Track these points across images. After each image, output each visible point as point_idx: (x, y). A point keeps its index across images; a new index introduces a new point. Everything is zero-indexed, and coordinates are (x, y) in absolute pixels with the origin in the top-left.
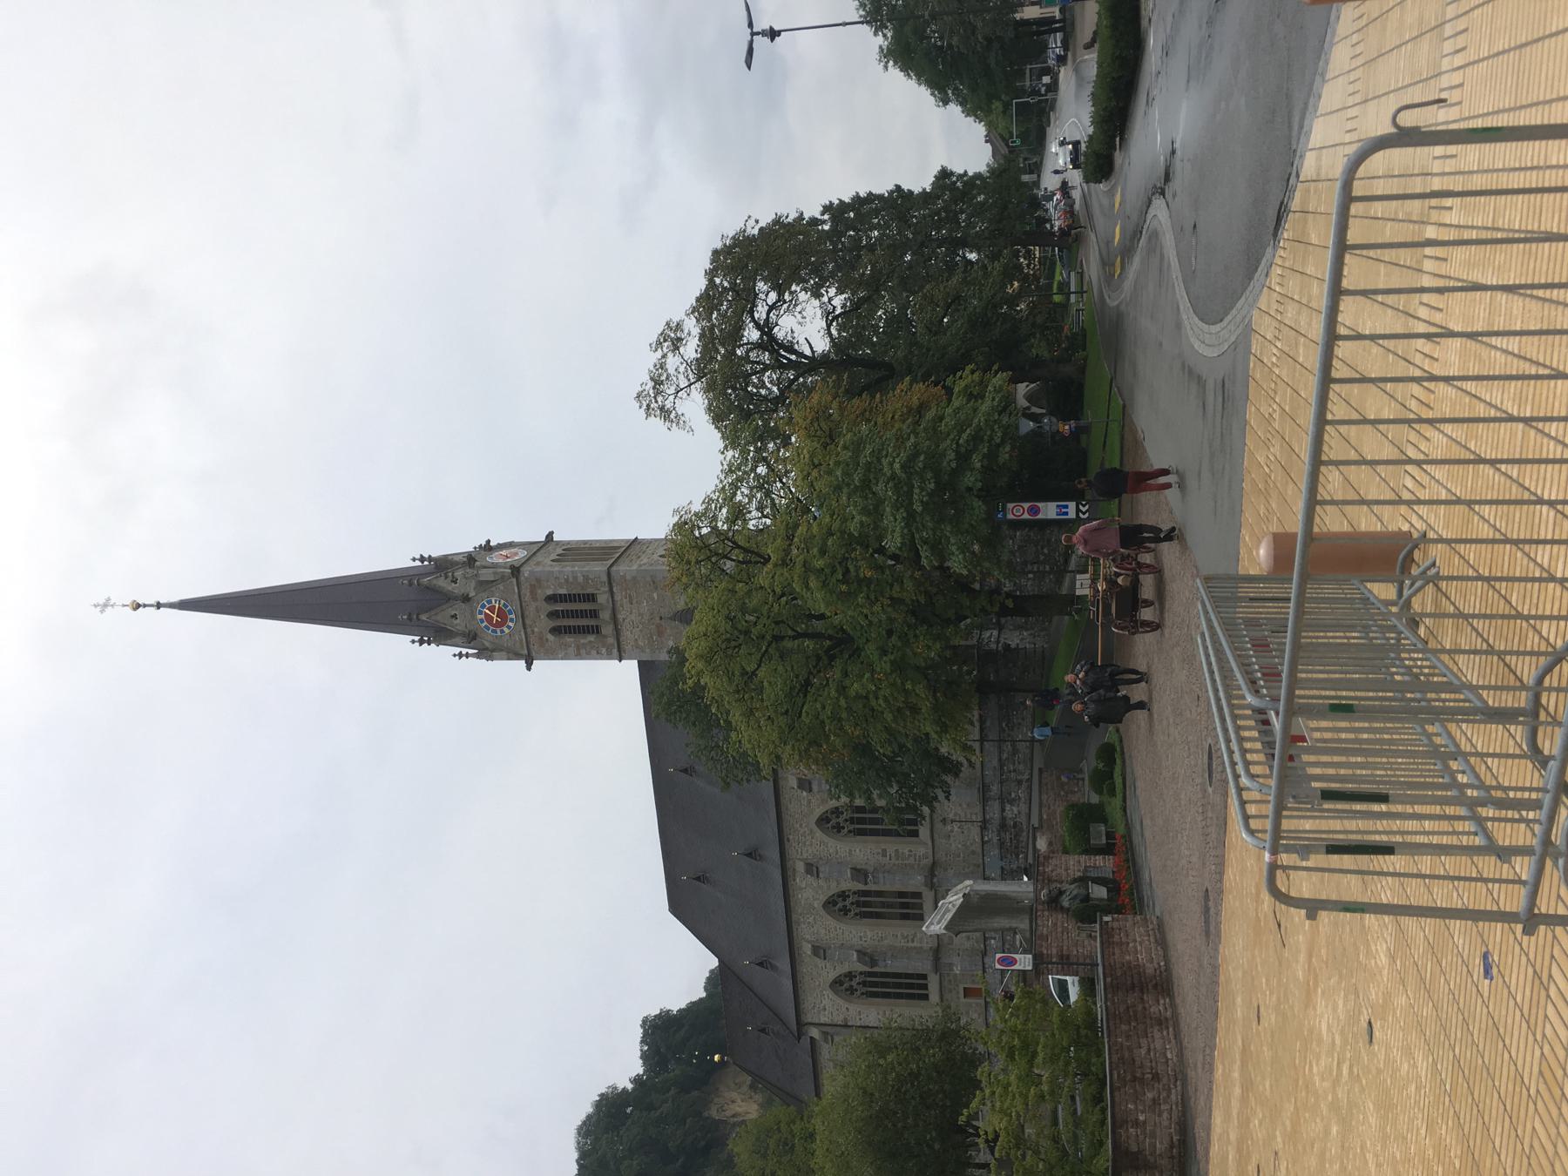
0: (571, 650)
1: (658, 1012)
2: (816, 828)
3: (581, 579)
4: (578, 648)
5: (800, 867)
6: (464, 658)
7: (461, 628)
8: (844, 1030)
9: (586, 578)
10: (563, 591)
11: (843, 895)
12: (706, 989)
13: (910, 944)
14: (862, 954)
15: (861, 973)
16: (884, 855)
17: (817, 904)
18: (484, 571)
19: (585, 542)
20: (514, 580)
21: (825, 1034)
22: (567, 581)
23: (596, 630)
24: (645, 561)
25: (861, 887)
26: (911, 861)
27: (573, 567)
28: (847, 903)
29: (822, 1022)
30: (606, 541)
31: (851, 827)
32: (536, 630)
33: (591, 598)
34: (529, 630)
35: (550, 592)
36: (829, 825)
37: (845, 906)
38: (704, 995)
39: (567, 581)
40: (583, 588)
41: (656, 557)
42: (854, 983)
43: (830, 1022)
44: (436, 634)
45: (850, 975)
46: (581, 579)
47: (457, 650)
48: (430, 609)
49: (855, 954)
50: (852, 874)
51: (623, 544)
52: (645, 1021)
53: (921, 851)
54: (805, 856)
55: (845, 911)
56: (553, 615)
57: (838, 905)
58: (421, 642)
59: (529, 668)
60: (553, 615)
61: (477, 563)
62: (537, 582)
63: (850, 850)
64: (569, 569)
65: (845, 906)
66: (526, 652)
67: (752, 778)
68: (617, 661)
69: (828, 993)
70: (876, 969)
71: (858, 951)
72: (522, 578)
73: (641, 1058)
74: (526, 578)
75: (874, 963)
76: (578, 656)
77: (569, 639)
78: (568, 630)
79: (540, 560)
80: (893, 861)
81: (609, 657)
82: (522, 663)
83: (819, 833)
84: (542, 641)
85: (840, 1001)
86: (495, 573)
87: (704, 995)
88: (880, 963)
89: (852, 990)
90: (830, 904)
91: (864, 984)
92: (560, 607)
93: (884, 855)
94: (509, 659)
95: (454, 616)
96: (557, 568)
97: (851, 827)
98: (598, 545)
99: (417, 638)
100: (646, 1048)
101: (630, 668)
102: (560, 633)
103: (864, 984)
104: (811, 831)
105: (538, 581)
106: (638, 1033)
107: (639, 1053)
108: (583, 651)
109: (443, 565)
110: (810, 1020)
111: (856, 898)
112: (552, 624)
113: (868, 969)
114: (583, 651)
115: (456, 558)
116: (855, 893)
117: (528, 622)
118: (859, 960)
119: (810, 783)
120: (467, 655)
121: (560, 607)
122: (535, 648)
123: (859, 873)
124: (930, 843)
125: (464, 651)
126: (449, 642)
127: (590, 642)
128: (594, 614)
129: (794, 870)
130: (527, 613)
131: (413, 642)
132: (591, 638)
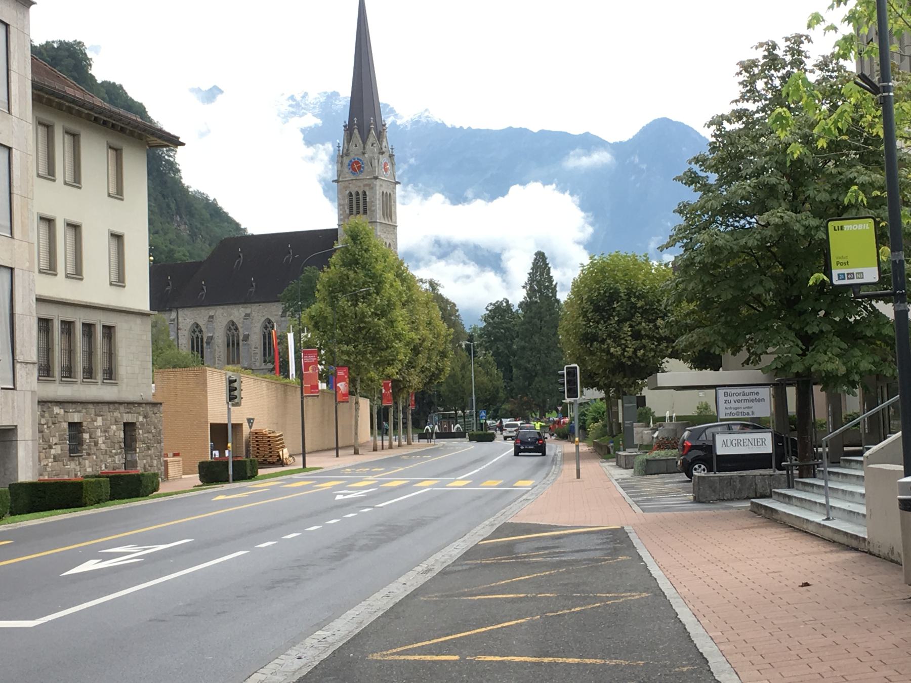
0: (342, 202)
1: (89, 56)
2: (266, 317)
3: (373, 208)
4: (343, 205)
5: (248, 311)
6: (337, 148)
7: (351, 149)
8: (176, 328)
9: (374, 211)
10: (367, 198)
11: (237, 329)
12: (104, 83)
13: (217, 359)
14: (212, 338)
15: (202, 336)
16: (255, 348)
17: (232, 318)
18: (376, 161)
19: (395, 202)
20: (372, 177)
21: (173, 320)
22: (372, 202)
23: (351, 213)
24: (382, 236)
25: (241, 338)
26: (253, 360)
27: (379, 204)
28: (233, 331)
29: (179, 318)
30: (395, 212)
31: (267, 333)
32: (351, 185)
33: (365, 212)
34: (350, 182)
35: (367, 193)
36: (267, 324)
37: (232, 330)
38: (99, 81)
39: (372, 202)
40: (369, 209)
41: (385, 240)
42: (197, 333)
43: (179, 321)
44: (349, 129)
45: (201, 331)
46: (373, 208)
47: (341, 145)
48: (359, 131)
49: (211, 335)
50: (246, 335)
51: (393, 221)
52: (79, 43)
53: (258, 364)
54: (253, 313)
55: (230, 329)
56: (357, 194)
57: (232, 326)
58: (345, 127)
59: (333, 181)
60: (357, 194)
61: (381, 156)
62: (372, 187)
63: (256, 333)
64: (378, 202)
65: (232, 330)
66: (341, 180)
67: (284, 306)
68: (337, 222)
69: (192, 322)
70: (205, 345)
71: (212, 336)
72: (373, 180)
73: (47, 43)
74: (373, 183)
75: (208, 343)
76: (339, 205)
77: (347, 201)
78: (351, 201)
79: (384, 185)
80: (253, 352)
81: (340, 220)
82: (336, 178)
83: (263, 319)
84: (346, 188)
85: (189, 327)
86: (375, 167)
87: (99, 81)
88: (208, 347)
89: (194, 332)
90: (233, 323)
91: (197, 338)
92: (361, 197)
93: (255, 348)
94: (337, 171)
95: (356, 146)
96: (378, 196)
97: (267, 333)
98: (393, 208)
99: (347, 123)
100: (55, 45)
101: (337, 227)
102: (350, 196)
103: (197, 338)
104: (264, 316)
105: (372, 188)
106: (70, 39)
107: (50, 40)
108: (341, 207)
109: (380, 135)
110: (179, 313)
111: (236, 335)
112: (353, 193)
113: (205, 340)
114: (341, 207)
115: (384, 144)
116: (238, 334)
117: (354, 181)
118: (208, 337)
119: (285, 316)
120: (339, 150)
121: (361, 197)
122: (342, 184)
123: (246, 338)
124: (261, 368)
125: (341, 149)
126: (345, 141)
127: (345, 211)
128: (358, 213)
129: (246, 308)
130: (358, 181)
131: (345, 122)
132: (348, 211)
